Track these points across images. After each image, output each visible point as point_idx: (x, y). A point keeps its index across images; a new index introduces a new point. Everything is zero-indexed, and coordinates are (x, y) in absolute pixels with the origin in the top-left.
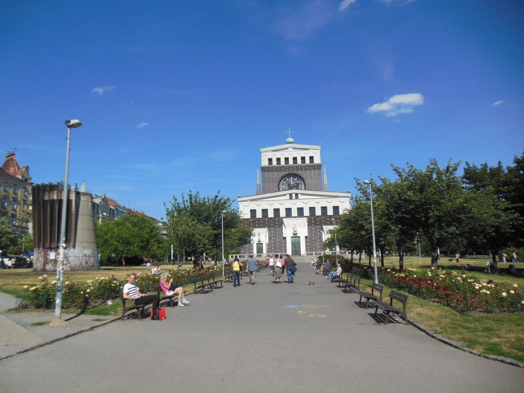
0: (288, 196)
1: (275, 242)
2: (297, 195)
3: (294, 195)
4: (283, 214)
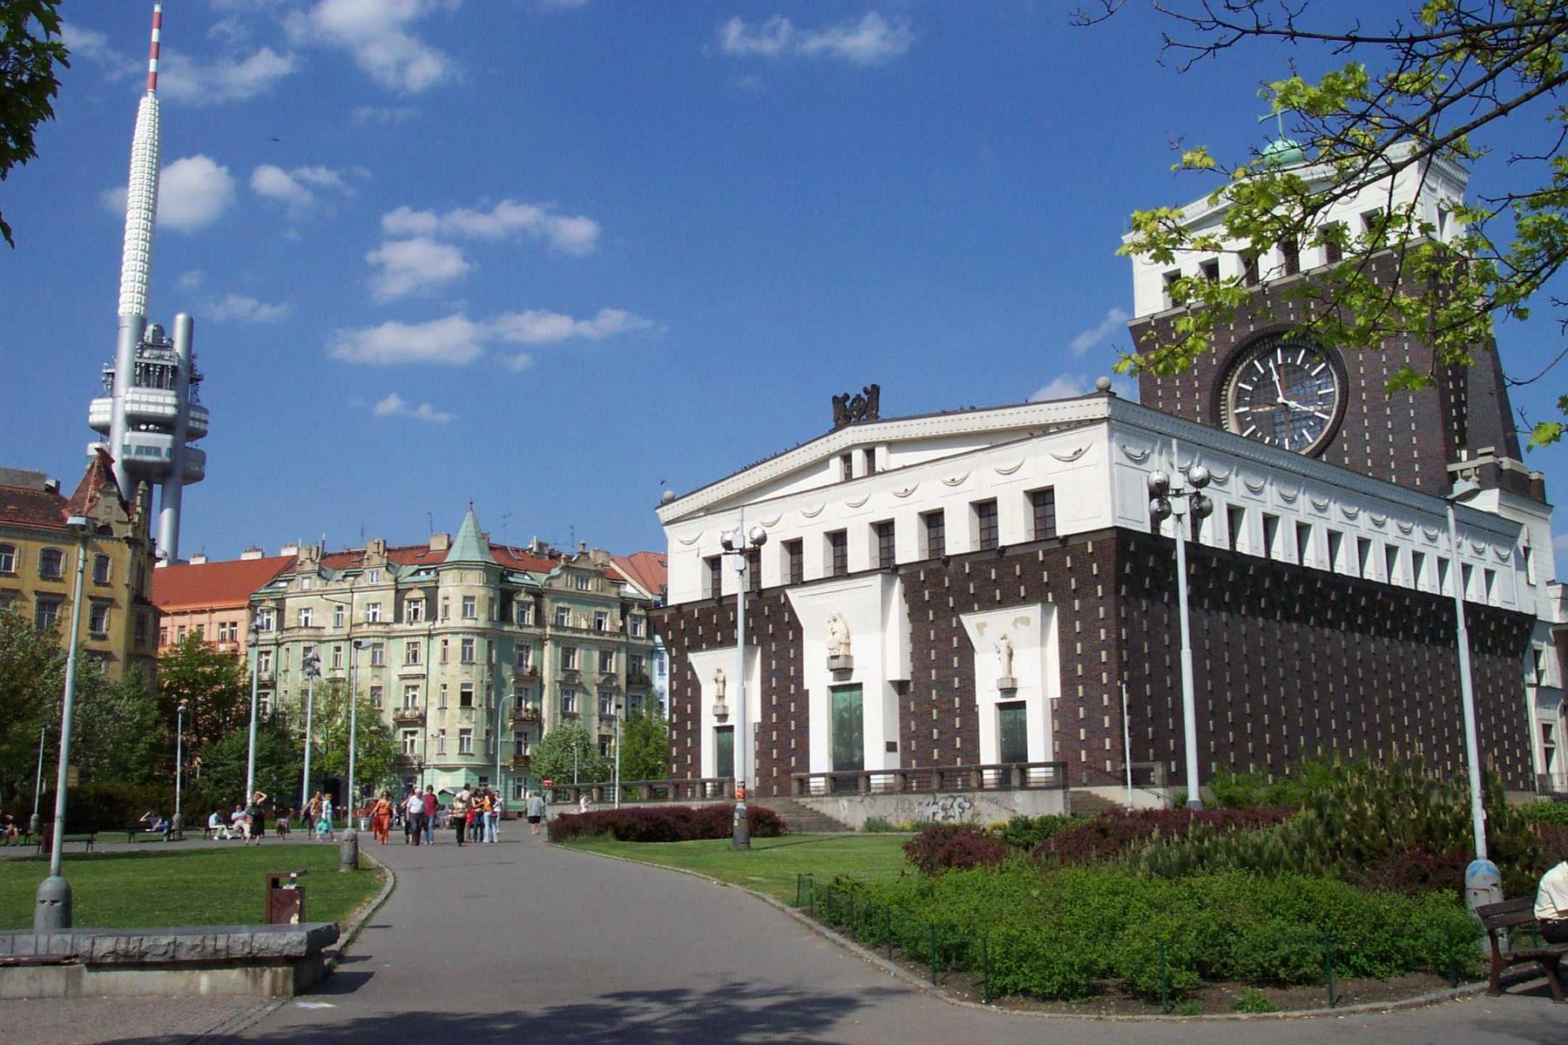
0: (836, 463)
1: (784, 718)
2: (870, 453)
3: (858, 457)
4: (816, 561)
